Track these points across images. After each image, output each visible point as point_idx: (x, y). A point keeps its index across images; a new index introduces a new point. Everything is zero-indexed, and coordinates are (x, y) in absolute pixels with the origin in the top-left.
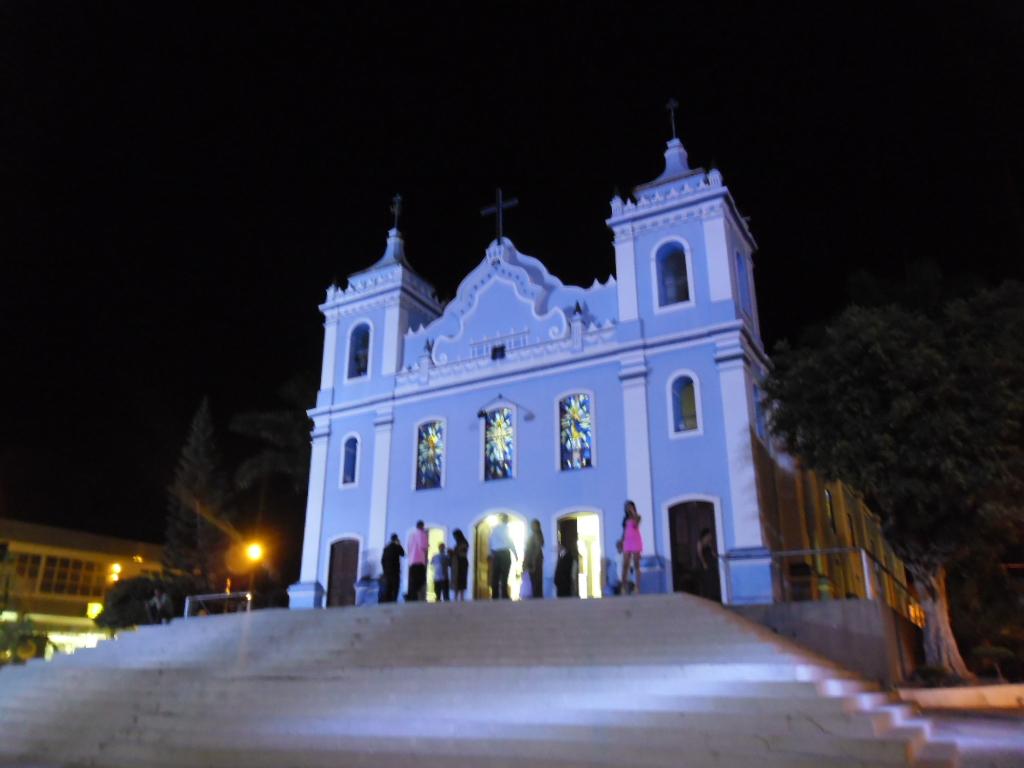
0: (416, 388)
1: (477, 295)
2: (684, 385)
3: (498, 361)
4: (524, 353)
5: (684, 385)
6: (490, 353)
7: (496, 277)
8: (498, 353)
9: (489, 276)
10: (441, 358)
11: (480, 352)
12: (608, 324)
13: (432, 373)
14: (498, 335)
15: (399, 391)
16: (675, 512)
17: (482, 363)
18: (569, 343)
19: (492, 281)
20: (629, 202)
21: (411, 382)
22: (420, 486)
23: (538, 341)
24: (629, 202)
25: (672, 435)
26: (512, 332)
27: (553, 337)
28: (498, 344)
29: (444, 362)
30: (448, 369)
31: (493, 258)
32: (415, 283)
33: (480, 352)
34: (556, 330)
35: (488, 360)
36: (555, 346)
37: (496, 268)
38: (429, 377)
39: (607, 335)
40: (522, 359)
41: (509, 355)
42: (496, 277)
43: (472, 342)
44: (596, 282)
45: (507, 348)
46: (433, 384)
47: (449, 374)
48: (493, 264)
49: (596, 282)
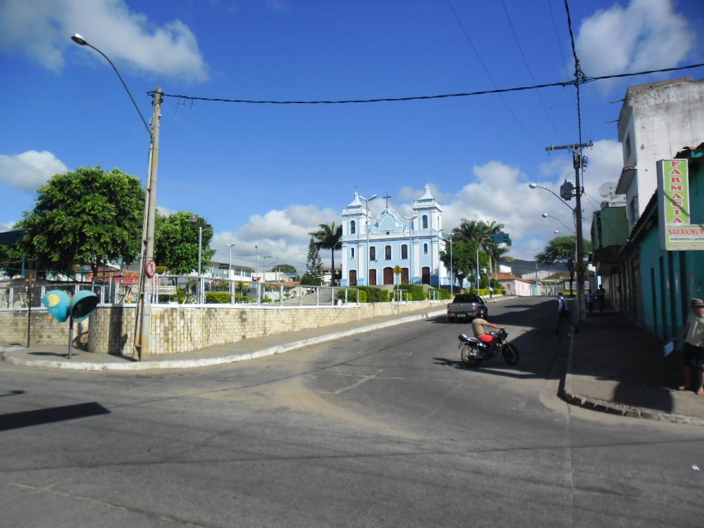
2: (426, 245)
5: (426, 245)
8: (388, 233)
14: (388, 229)
16: (423, 268)
26: (391, 229)
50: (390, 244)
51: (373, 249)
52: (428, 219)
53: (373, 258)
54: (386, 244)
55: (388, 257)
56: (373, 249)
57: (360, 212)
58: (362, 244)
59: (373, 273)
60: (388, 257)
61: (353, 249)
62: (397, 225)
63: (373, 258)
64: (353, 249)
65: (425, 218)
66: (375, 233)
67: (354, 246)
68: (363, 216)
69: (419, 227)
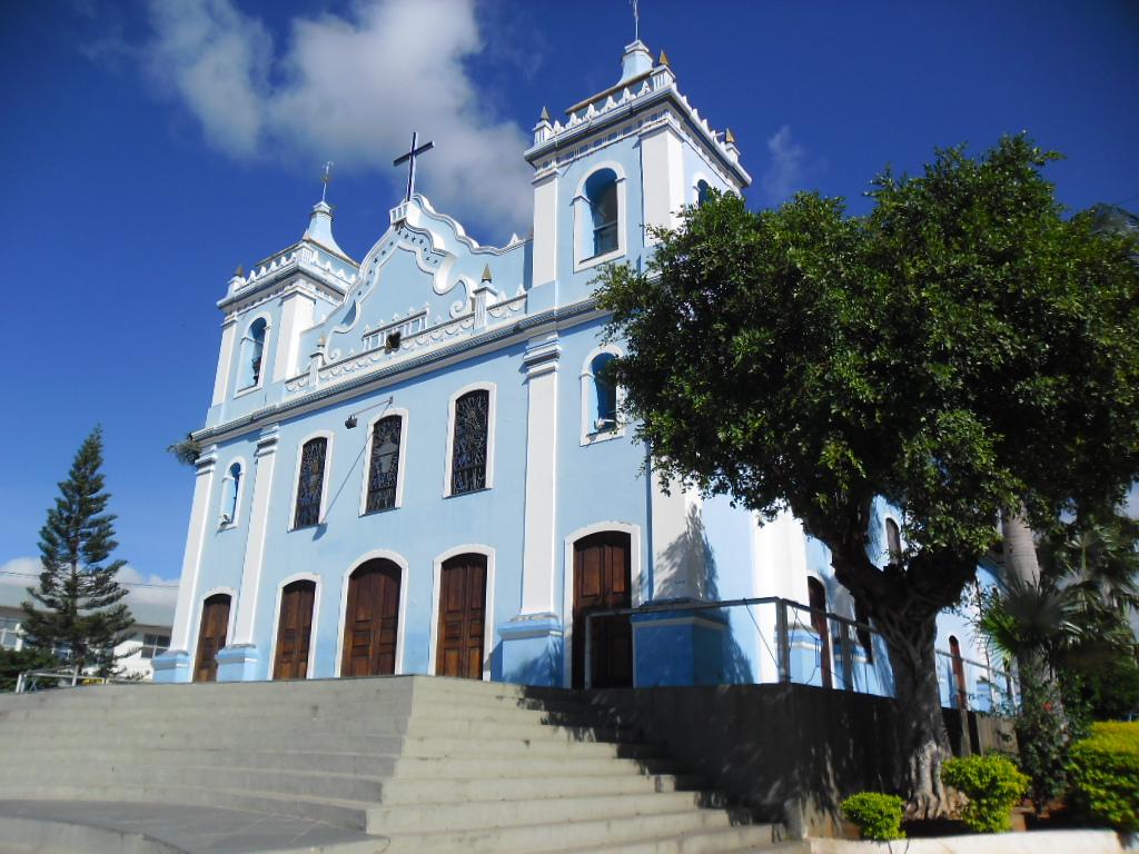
1: (377, 271)
7: (401, 242)
8: (394, 342)
12: (521, 291)
13: (324, 374)
14: (397, 317)
15: (287, 399)
17: (375, 356)
18: (471, 321)
19: (395, 247)
20: (557, 123)
23: (440, 320)
24: (557, 123)
25: (588, 441)
26: (413, 311)
27: (456, 316)
28: (393, 332)
29: (335, 361)
31: (398, 219)
32: (328, 265)
34: (460, 304)
35: (383, 350)
36: (456, 326)
39: (519, 305)
41: (405, 345)
43: (369, 329)
44: (515, 236)
45: (404, 335)
49: (515, 236)
50: (401, 403)
51: (315, 450)
52: (621, 189)
54: (371, 412)
55: (382, 494)
56: (315, 450)
57: (292, 266)
58: (279, 432)
60: (382, 494)
61: (236, 470)
62: (442, 281)
64: (236, 470)
65: (602, 191)
66: (338, 355)
67: (241, 453)
68: (301, 284)
69: (566, 249)
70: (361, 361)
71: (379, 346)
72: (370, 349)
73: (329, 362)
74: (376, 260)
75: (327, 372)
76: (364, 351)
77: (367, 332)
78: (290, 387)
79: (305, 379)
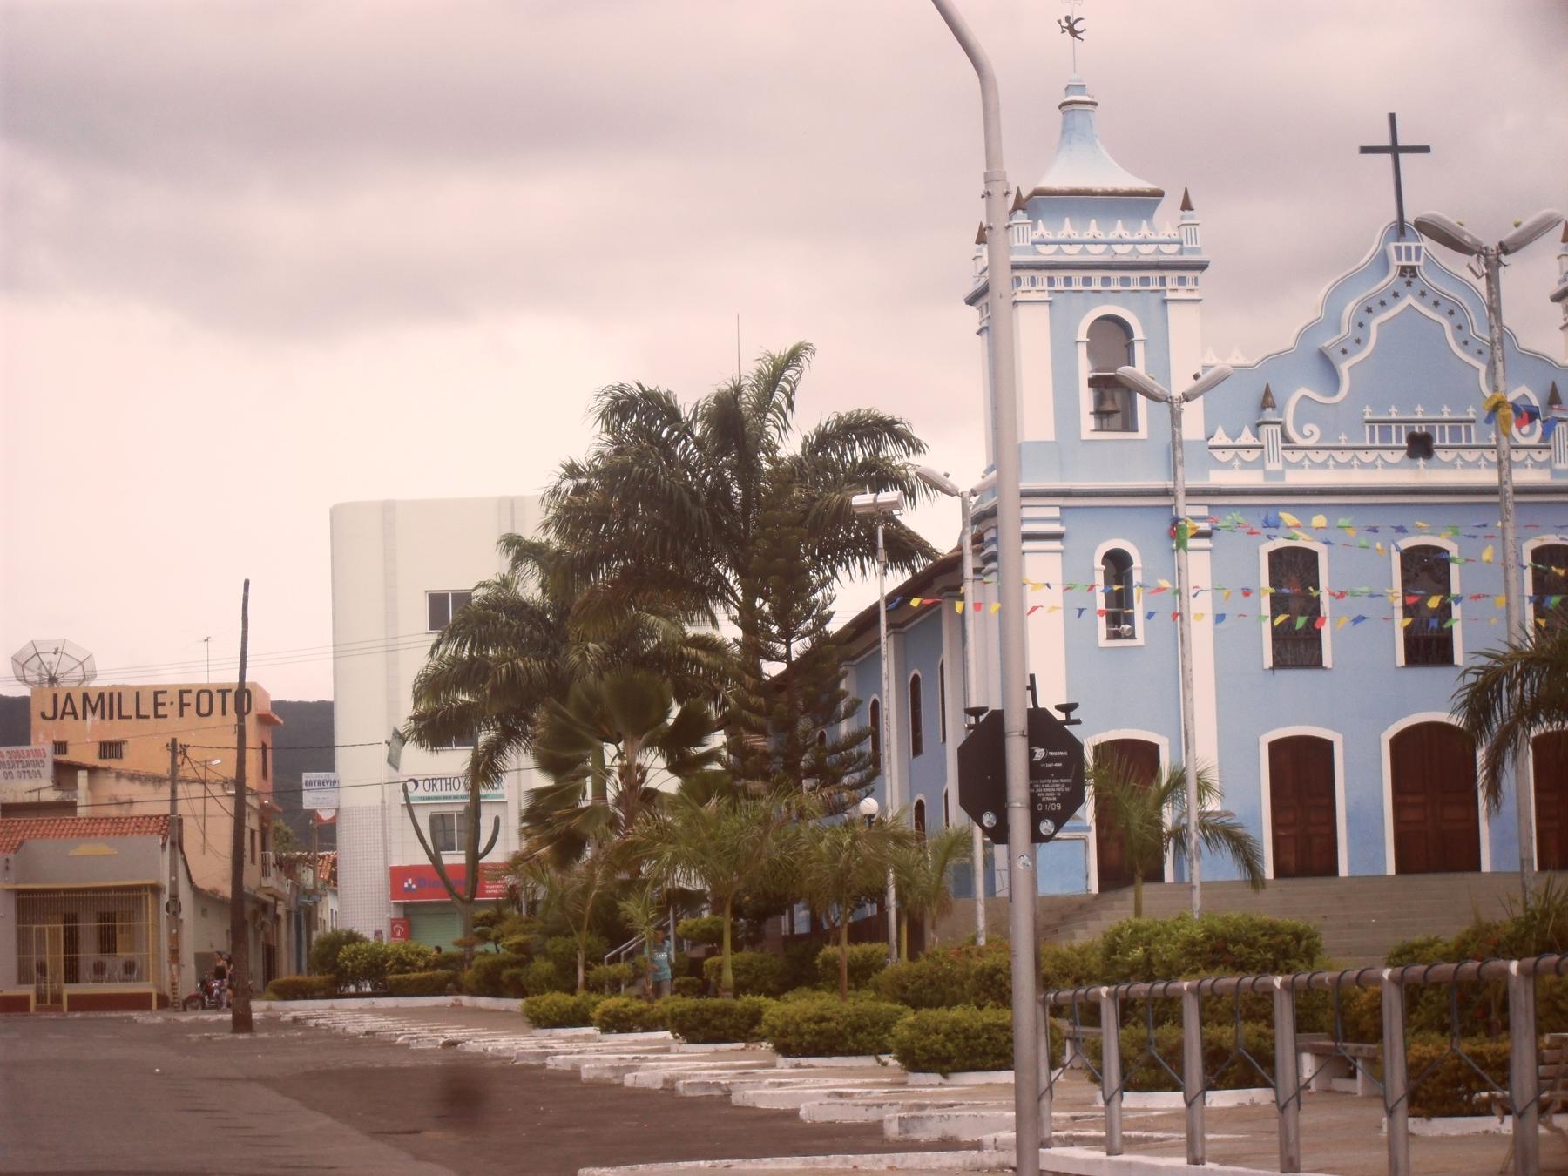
0: (1254, 479)
1: (1374, 324)
3: (1421, 462)
4: (1471, 456)
6: (1404, 444)
7: (1409, 299)
8: (1420, 446)
9: (1396, 295)
10: (1307, 433)
11: (1385, 436)
15: (1218, 479)
17: (1387, 455)
18: (1544, 456)
21: (1246, 465)
22: (1280, 663)
27: (1523, 441)
29: (1310, 443)
30: (1323, 455)
31: (1404, 263)
33: (1385, 436)
35: (1400, 455)
37: (1409, 284)
38: (1288, 464)
40: (1468, 465)
41: (1440, 454)
42: (1409, 299)
45: (1437, 443)
46: (1294, 479)
47: (1324, 465)
48: (1404, 269)
51: (1293, 568)
53: (1297, 646)
56: (1293, 568)
59: (1302, 770)
61: (1118, 563)
63: (1297, 646)
66: (1312, 434)
70: (1369, 457)
71: (1394, 444)
72: (1377, 444)
73: (1301, 442)
74: (1369, 310)
75: (1299, 455)
76: (1368, 444)
77: (1368, 417)
78: (1217, 454)
79: (1255, 454)
